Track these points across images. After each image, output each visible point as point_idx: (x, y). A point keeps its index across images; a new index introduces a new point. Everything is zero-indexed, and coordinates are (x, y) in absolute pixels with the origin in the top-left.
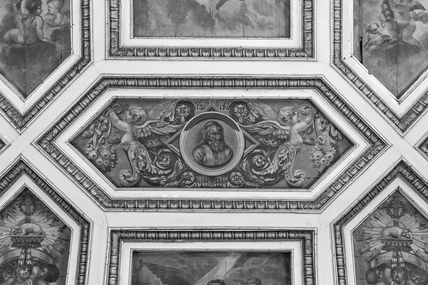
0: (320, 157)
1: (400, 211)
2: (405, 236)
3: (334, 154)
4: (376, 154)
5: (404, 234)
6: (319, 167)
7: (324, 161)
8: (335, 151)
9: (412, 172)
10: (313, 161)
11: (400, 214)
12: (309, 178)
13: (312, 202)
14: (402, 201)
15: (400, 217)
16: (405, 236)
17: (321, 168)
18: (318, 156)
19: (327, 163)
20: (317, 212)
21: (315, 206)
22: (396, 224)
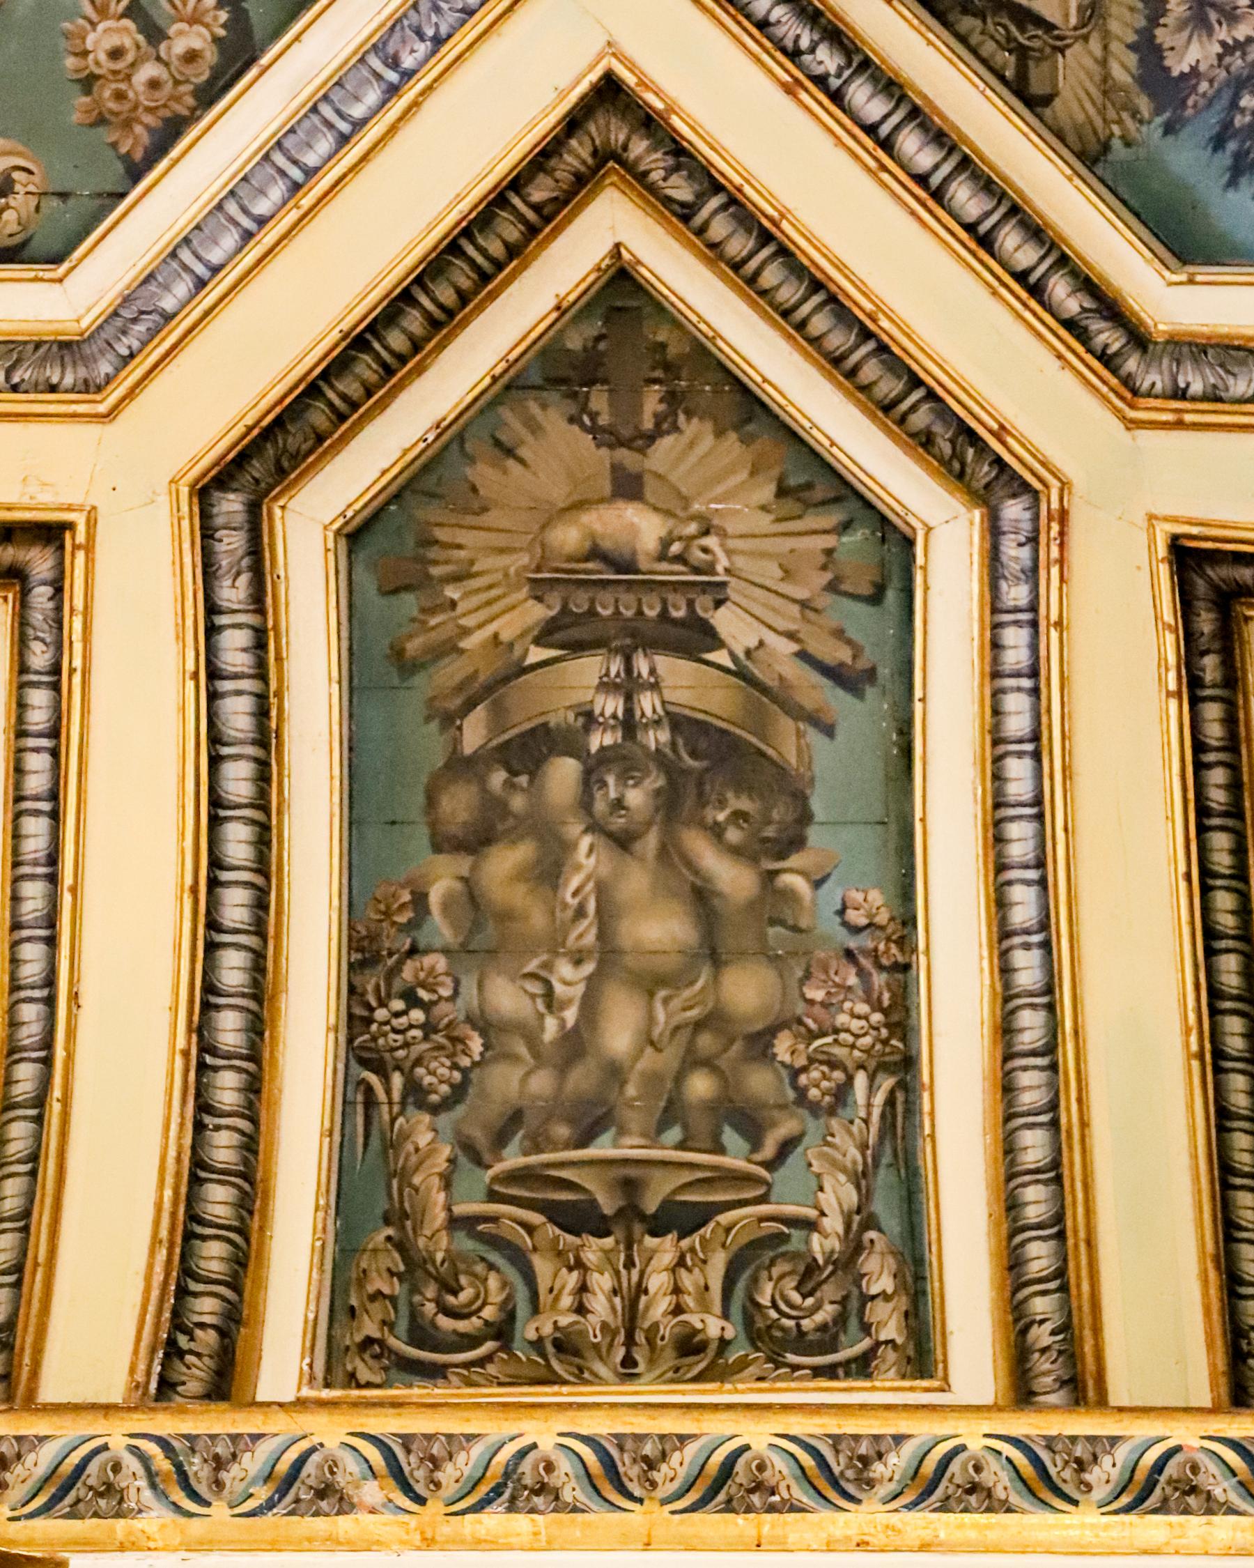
0: (130, 57)
1: (652, 402)
2: (680, 559)
3: (216, 40)
4: (450, 36)
5: (676, 548)
6: (127, 124)
7: (154, 84)
8: (223, 16)
9: (681, 154)
10: (88, 83)
11: (648, 424)
12: (63, 196)
13: (65, 345)
14: (661, 337)
15: (651, 438)
16: (680, 559)
17: (138, 129)
18: (116, 54)
19: (178, 99)
20: (81, 408)
21: (82, 372)
22: (628, 487)
